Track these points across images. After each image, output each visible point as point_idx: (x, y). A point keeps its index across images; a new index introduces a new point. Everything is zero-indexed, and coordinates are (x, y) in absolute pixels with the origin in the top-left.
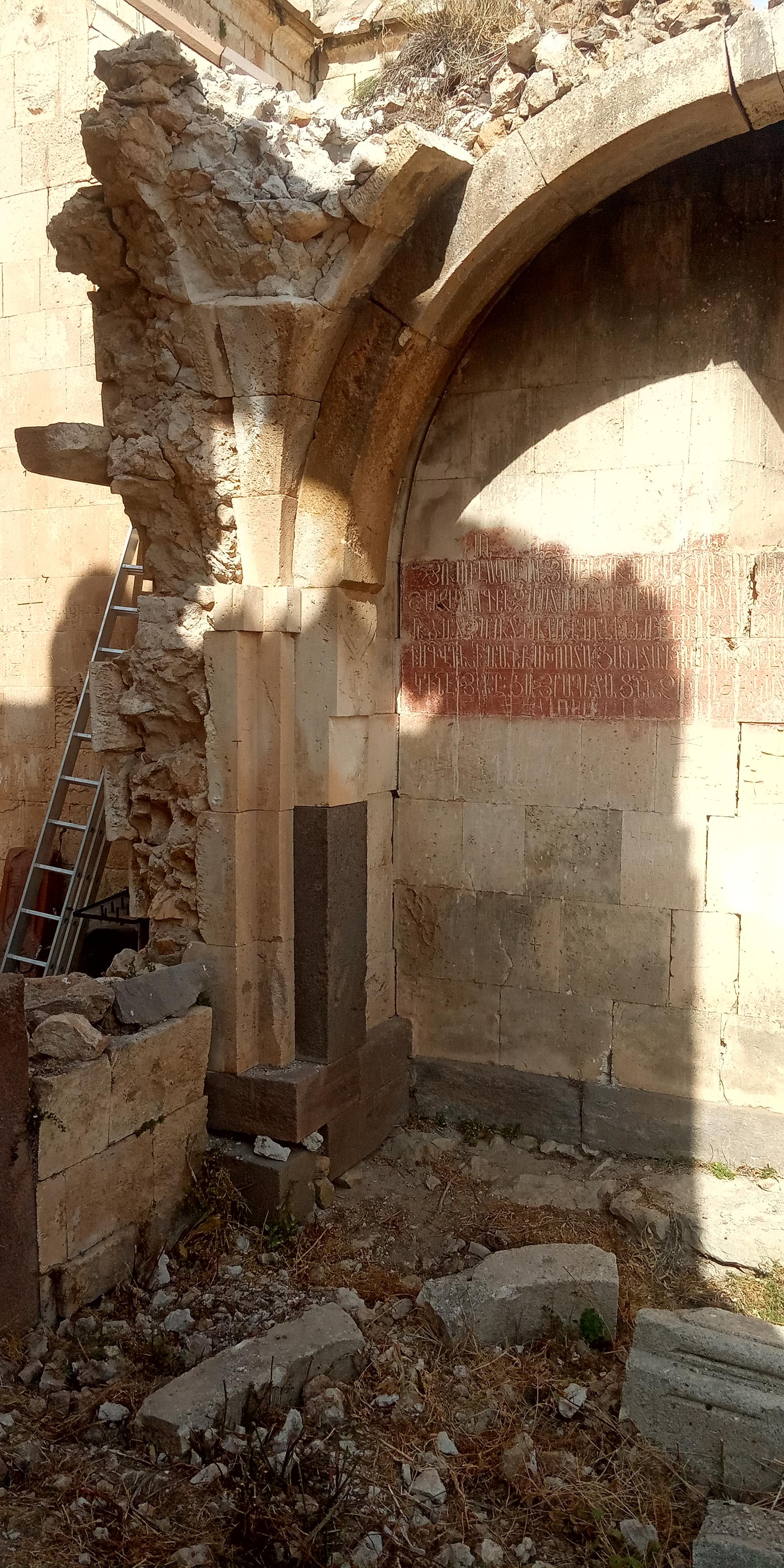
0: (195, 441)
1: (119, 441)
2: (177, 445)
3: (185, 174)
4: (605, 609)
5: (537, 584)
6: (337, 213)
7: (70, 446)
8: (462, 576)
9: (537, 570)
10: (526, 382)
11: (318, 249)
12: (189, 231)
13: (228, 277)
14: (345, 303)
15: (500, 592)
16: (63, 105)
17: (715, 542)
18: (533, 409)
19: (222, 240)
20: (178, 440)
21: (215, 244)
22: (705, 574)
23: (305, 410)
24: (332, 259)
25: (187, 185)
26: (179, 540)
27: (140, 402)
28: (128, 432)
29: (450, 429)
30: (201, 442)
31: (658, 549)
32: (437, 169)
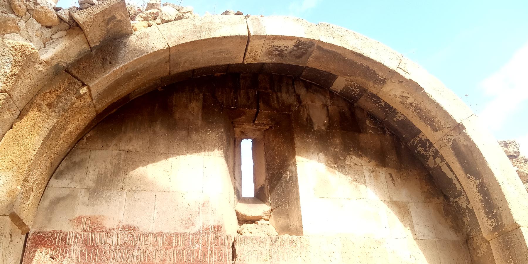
4: (158, 262)
5: (118, 247)
6: (66, 17)
8: (70, 240)
9: (119, 239)
10: (123, 148)
11: (47, 33)
14: (54, 63)
15: (94, 251)
17: (216, 229)
18: (125, 160)
22: (211, 245)
23: (12, 110)
24: (54, 40)
29: (75, 164)
31: (187, 231)
32: (121, 21)
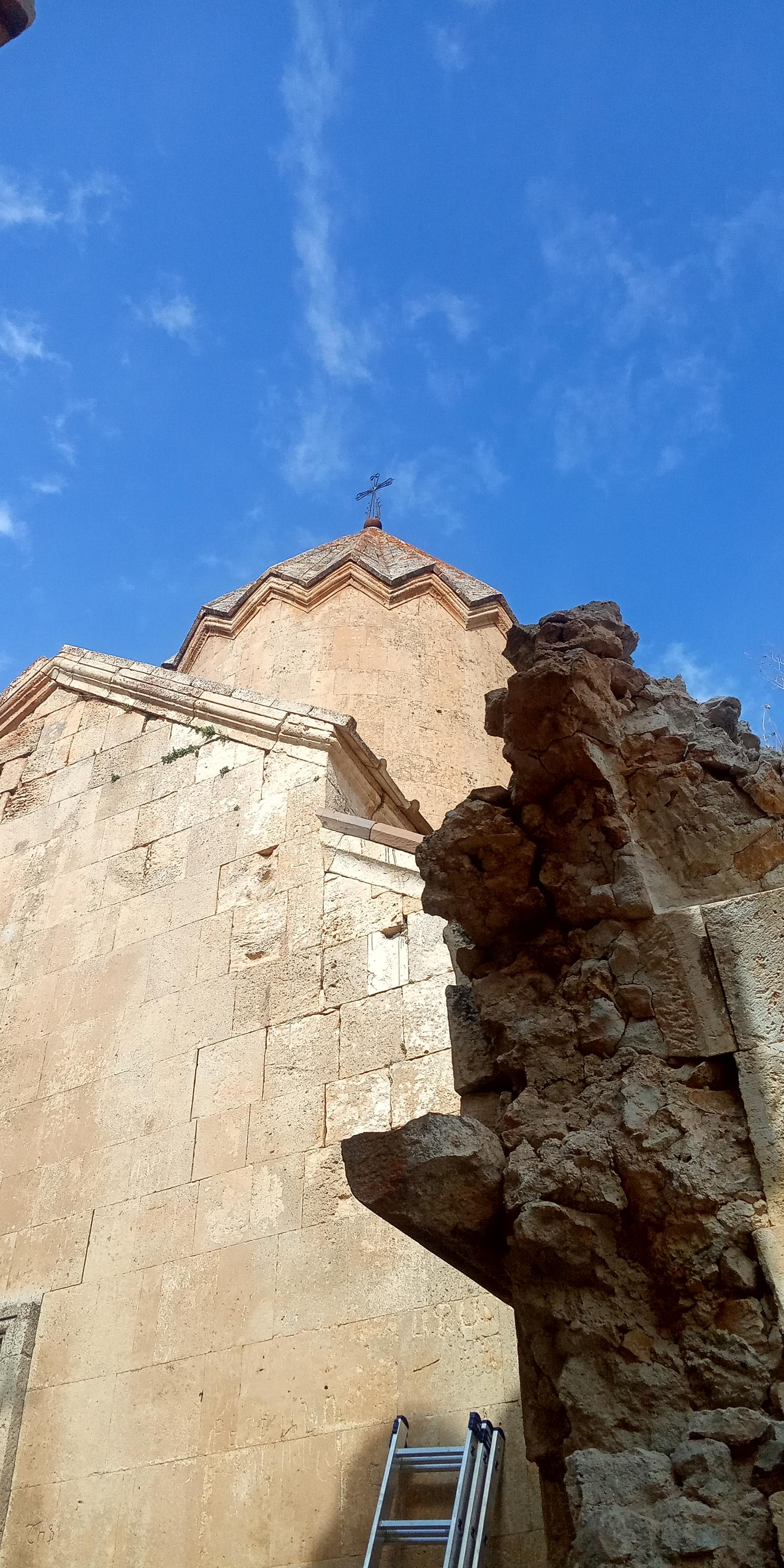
0: (672, 1132)
1: (525, 1149)
2: (640, 1138)
3: (649, 737)
7: (448, 1151)
12: (648, 817)
13: (710, 878)
16: (290, 945)
19: (706, 818)
20: (643, 1128)
21: (694, 828)
25: (648, 754)
26: (630, 1342)
27: (552, 1091)
28: (540, 1134)
30: (683, 1132)
